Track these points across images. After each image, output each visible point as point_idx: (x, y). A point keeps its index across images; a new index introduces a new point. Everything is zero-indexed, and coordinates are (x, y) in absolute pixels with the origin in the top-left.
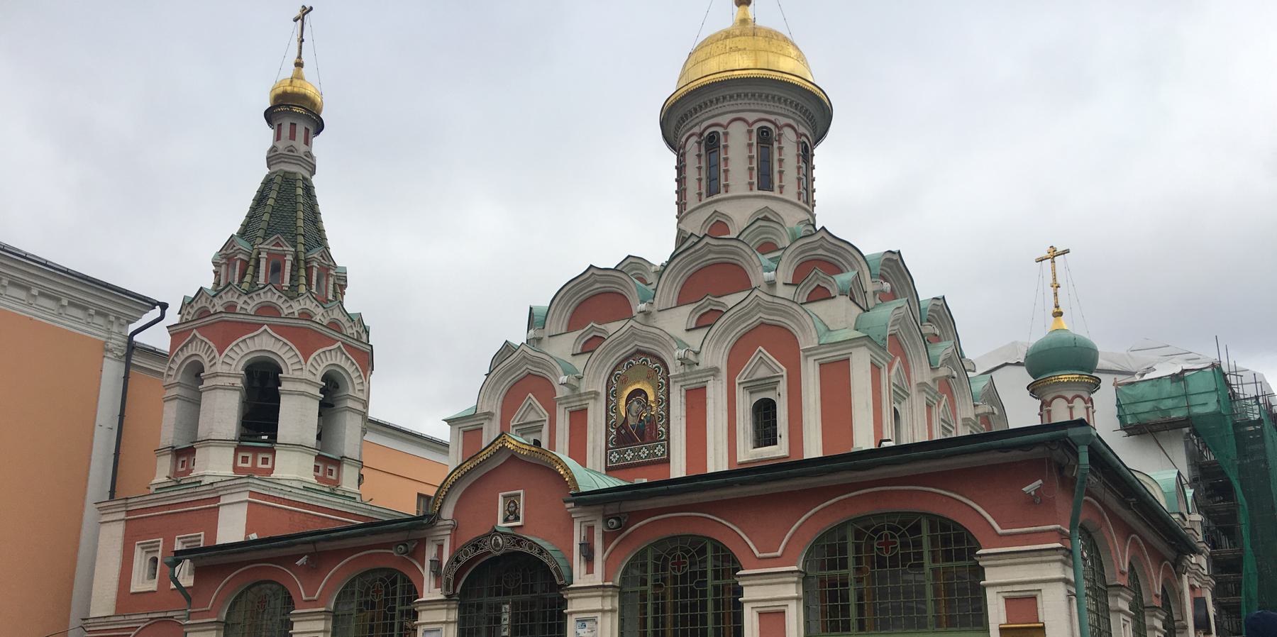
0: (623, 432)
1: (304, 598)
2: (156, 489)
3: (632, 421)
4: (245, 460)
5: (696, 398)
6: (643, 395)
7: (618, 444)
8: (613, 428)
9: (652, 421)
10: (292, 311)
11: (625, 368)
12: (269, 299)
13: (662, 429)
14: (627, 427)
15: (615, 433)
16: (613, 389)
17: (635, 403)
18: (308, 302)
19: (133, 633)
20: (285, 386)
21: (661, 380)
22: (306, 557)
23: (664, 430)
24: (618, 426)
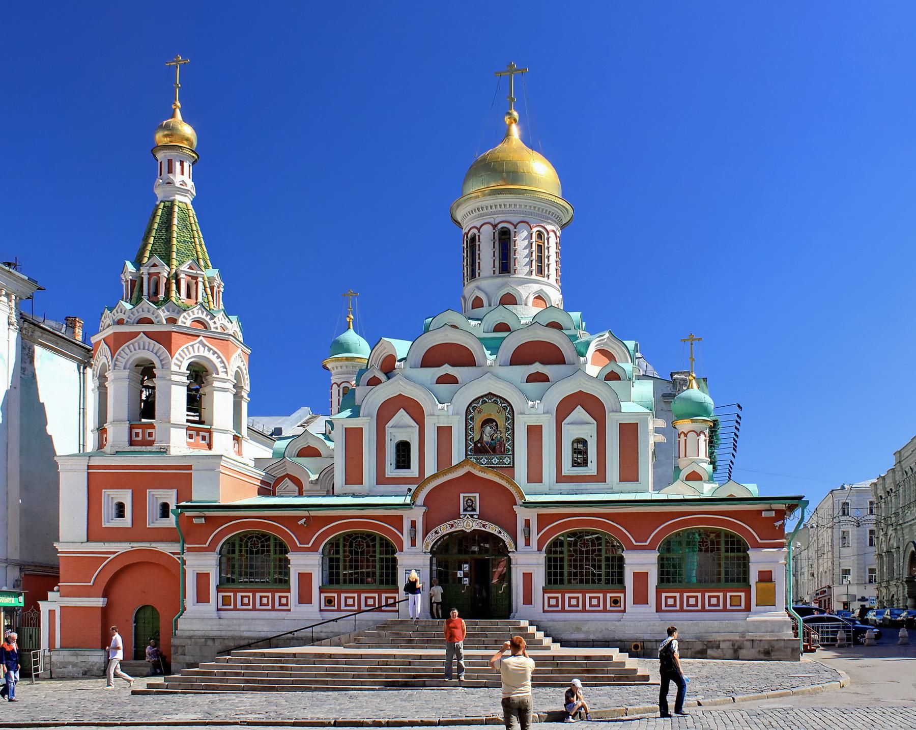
0: (479, 445)
1: (299, 545)
2: (117, 452)
3: (486, 438)
4: (191, 437)
5: (535, 432)
6: (494, 424)
7: (475, 453)
8: (471, 441)
9: (501, 442)
10: (216, 326)
11: (480, 403)
12: (200, 315)
13: (508, 447)
14: (481, 443)
15: (473, 445)
16: (471, 415)
17: (488, 427)
18: (223, 318)
19: (112, 556)
20: (216, 384)
21: (508, 415)
22: (305, 519)
23: (510, 448)
24: (475, 441)
